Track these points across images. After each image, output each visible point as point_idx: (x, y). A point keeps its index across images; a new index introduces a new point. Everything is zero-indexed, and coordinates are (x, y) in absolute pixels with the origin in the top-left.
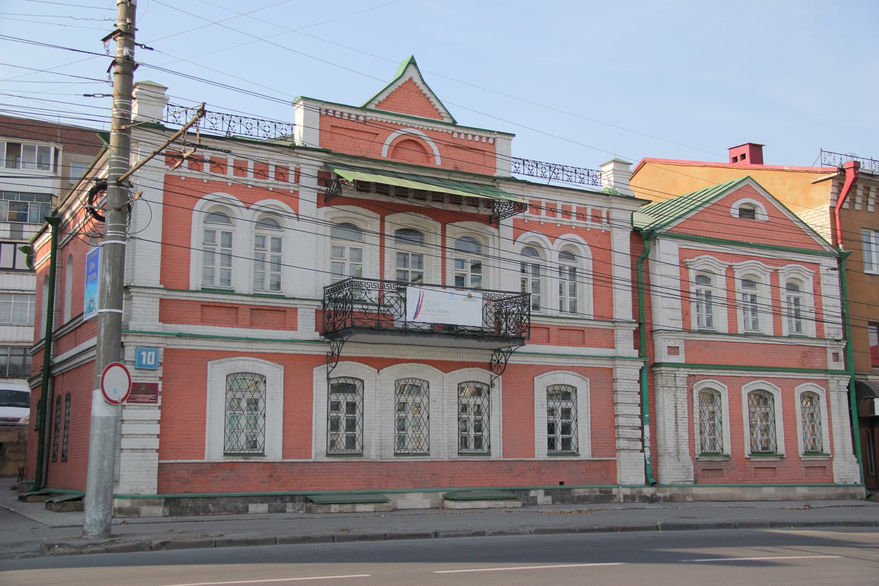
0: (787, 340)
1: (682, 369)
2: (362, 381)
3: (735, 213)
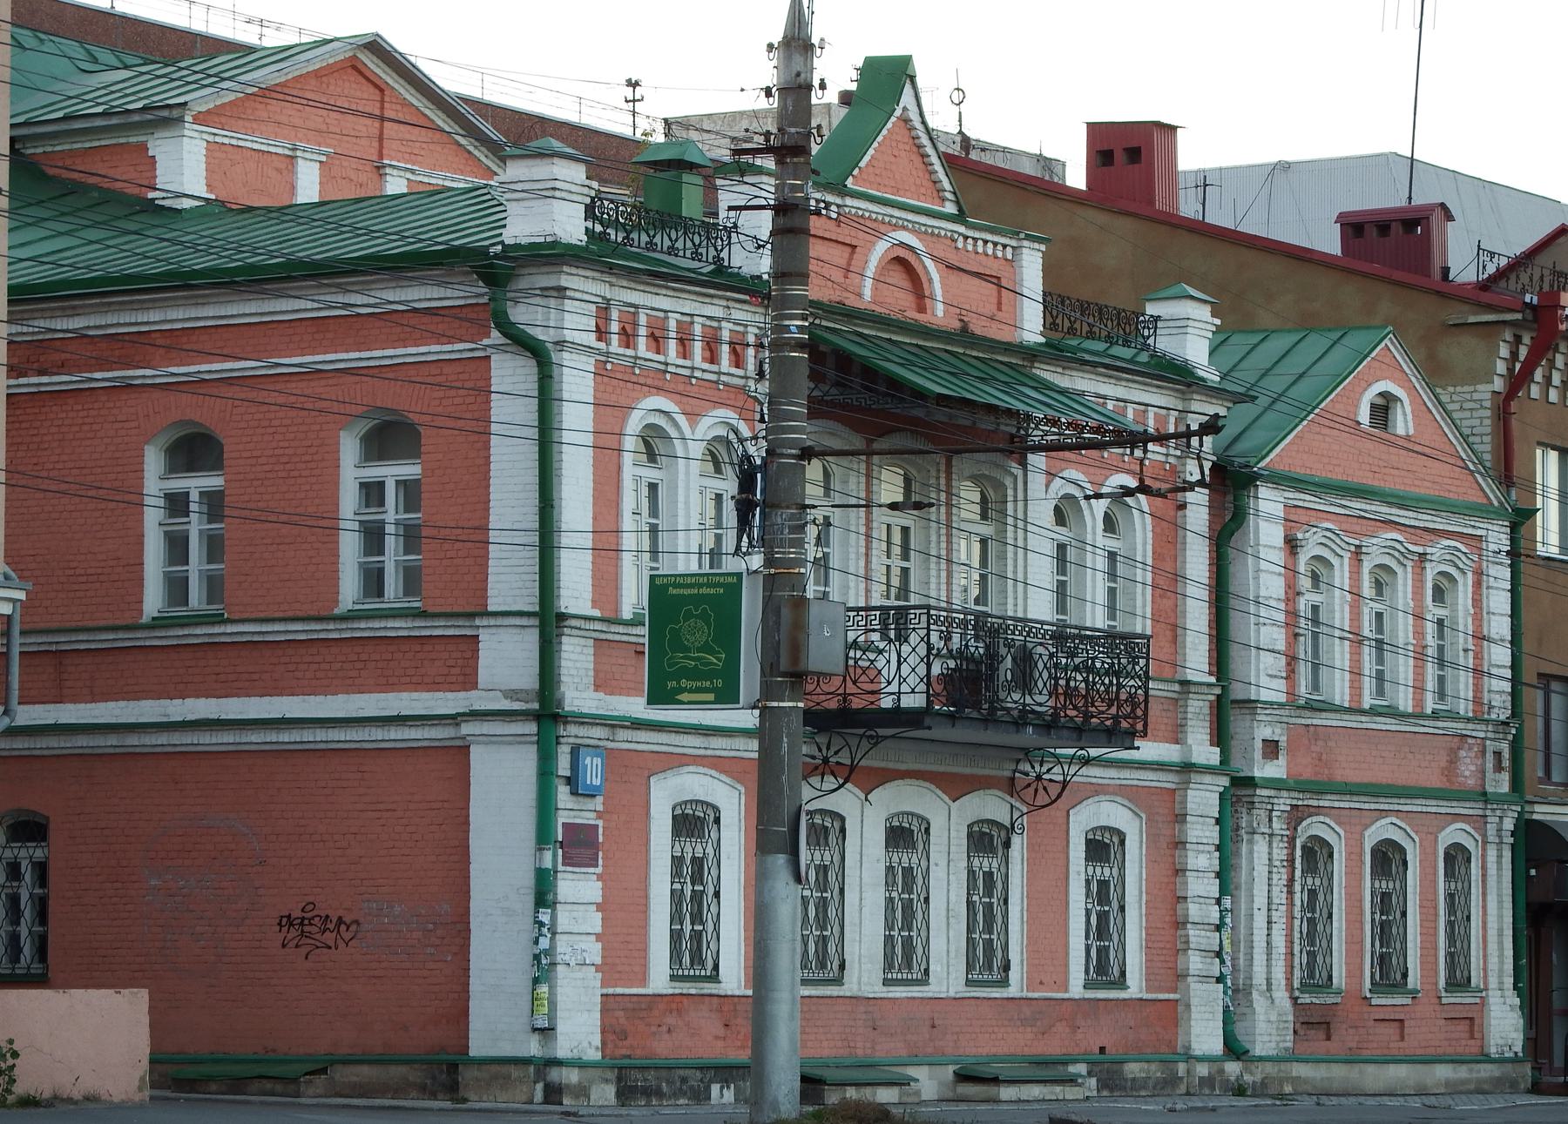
0: (1432, 723)
1: (1285, 794)
2: (843, 819)
3: (1364, 416)
